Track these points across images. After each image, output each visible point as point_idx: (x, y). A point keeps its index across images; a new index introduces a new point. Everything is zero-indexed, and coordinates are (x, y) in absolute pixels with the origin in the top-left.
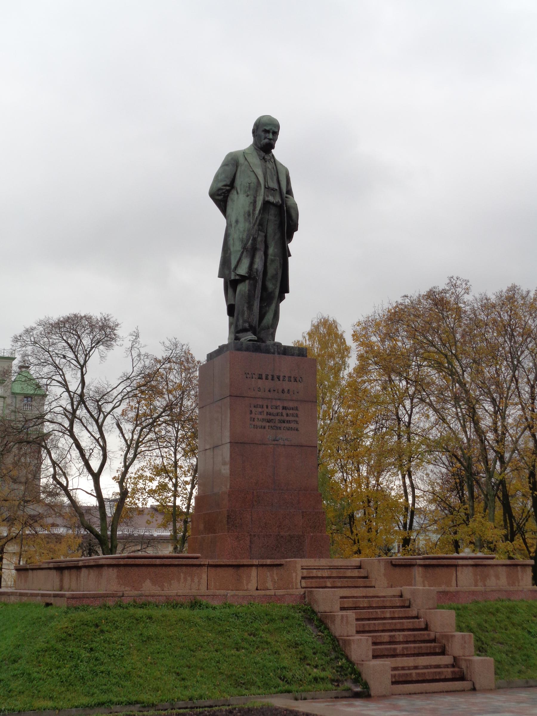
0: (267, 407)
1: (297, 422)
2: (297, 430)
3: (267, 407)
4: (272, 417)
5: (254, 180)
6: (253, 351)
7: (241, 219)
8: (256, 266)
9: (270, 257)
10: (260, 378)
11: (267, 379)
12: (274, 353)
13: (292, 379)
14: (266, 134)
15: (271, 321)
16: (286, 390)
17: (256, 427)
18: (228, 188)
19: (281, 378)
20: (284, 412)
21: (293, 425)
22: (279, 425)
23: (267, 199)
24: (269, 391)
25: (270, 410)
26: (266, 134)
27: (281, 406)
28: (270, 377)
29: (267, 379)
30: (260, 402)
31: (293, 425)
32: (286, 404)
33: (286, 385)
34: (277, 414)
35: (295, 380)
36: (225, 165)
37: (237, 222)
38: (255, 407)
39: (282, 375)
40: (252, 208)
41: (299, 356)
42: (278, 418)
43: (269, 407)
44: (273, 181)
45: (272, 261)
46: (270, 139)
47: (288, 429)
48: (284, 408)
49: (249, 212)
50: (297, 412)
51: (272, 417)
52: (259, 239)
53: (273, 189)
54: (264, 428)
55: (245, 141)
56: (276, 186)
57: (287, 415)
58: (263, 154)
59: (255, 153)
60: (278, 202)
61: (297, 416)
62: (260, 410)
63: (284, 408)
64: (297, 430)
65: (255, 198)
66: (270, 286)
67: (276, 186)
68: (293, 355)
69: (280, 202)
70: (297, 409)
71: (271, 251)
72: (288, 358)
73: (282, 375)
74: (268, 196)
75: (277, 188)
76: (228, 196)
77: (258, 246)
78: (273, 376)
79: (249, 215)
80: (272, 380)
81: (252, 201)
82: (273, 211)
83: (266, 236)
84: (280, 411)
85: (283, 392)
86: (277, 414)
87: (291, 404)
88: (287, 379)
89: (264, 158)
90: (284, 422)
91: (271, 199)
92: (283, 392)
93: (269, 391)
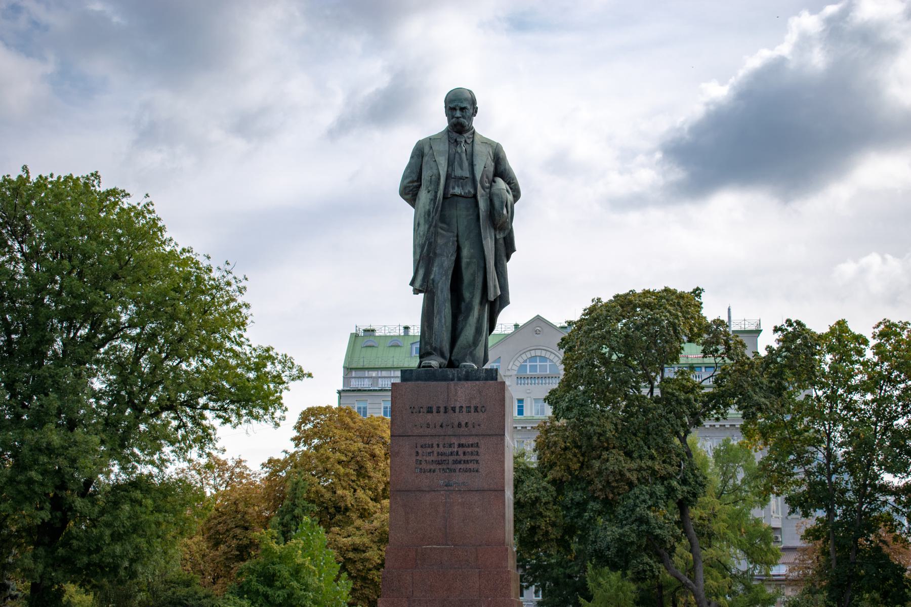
0: (438, 445)
1: (477, 462)
2: (477, 471)
3: (438, 445)
4: (444, 458)
5: (435, 171)
6: (426, 380)
7: (422, 222)
8: (432, 277)
9: (464, 261)
10: (430, 410)
11: (438, 412)
12: (452, 380)
13: (472, 410)
14: (460, 108)
15: (471, 338)
16: (463, 424)
17: (423, 471)
18: (415, 184)
19: (457, 410)
20: (461, 451)
21: (471, 466)
22: (453, 467)
23: (451, 191)
24: (441, 426)
25: (441, 449)
26: (460, 108)
27: (456, 443)
28: (442, 410)
29: (438, 412)
30: (428, 441)
31: (471, 466)
32: (463, 441)
33: (464, 418)
34: (452, 454)
35: (476, 410)
36: (412, 157)
37: (419, 224)
38: (422, 447)
39: (458, 405)
40: (432, 205)
41: (486, 379)
42: (451, 458)
43: (441, 446)
44: (462, 169)
45: (468, 264)
46: (458, 118)
47: (466, 471)
48: (460, 445)
49: (429, 211)
50: (476, 449)
51: (444, 458)
52: (440, 241)
53: (461, 178)
54: (434, 471)
55: (439, 123)
56: (467, 174)
57: (464, 453)
58: (455, 135)
59: (446, 136)
60: (469, 192)
61: (477, 454)
62: (429, 450)
63: (460, 445)
64: (477, 471)
65: (436, 193)
66: (467, 295)
67: (467, 174)
68: (478, 379)
69: (472, 191)
70: (477, 445)
71: (465, 252)
72: (469, 384)
73: (458, 405)
74: (453, 188)
75: (468, 175)
76: (417, 194)
77: (438, 251)
78: (446, 408)
79: (429, 215)
80: (446, 412)
81: (432, 197)
82: (462, 204)
83: (457, 236)
84: (455, 450)
85: (459, 425)
86: (452, 454)
87: (471, 441)
88: (464, 410)
89: (456, 141)
90: (460, 462)
91: (457, 191)
92: (459, 425)
93: (441, 426)
